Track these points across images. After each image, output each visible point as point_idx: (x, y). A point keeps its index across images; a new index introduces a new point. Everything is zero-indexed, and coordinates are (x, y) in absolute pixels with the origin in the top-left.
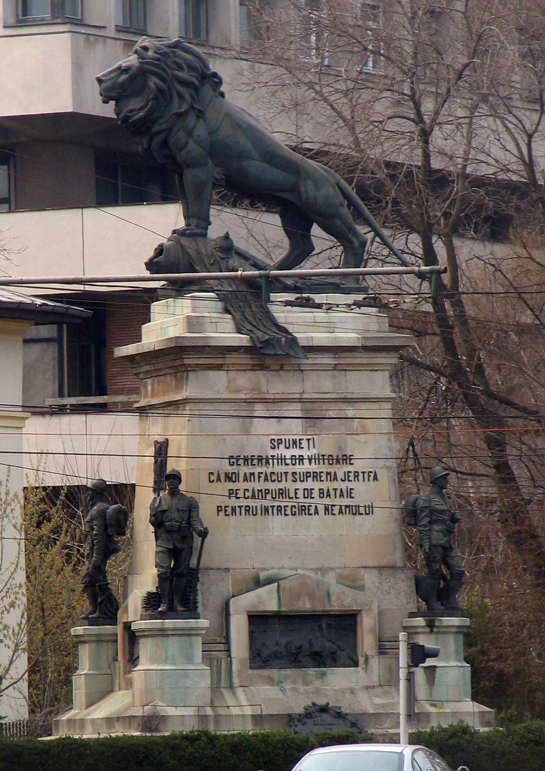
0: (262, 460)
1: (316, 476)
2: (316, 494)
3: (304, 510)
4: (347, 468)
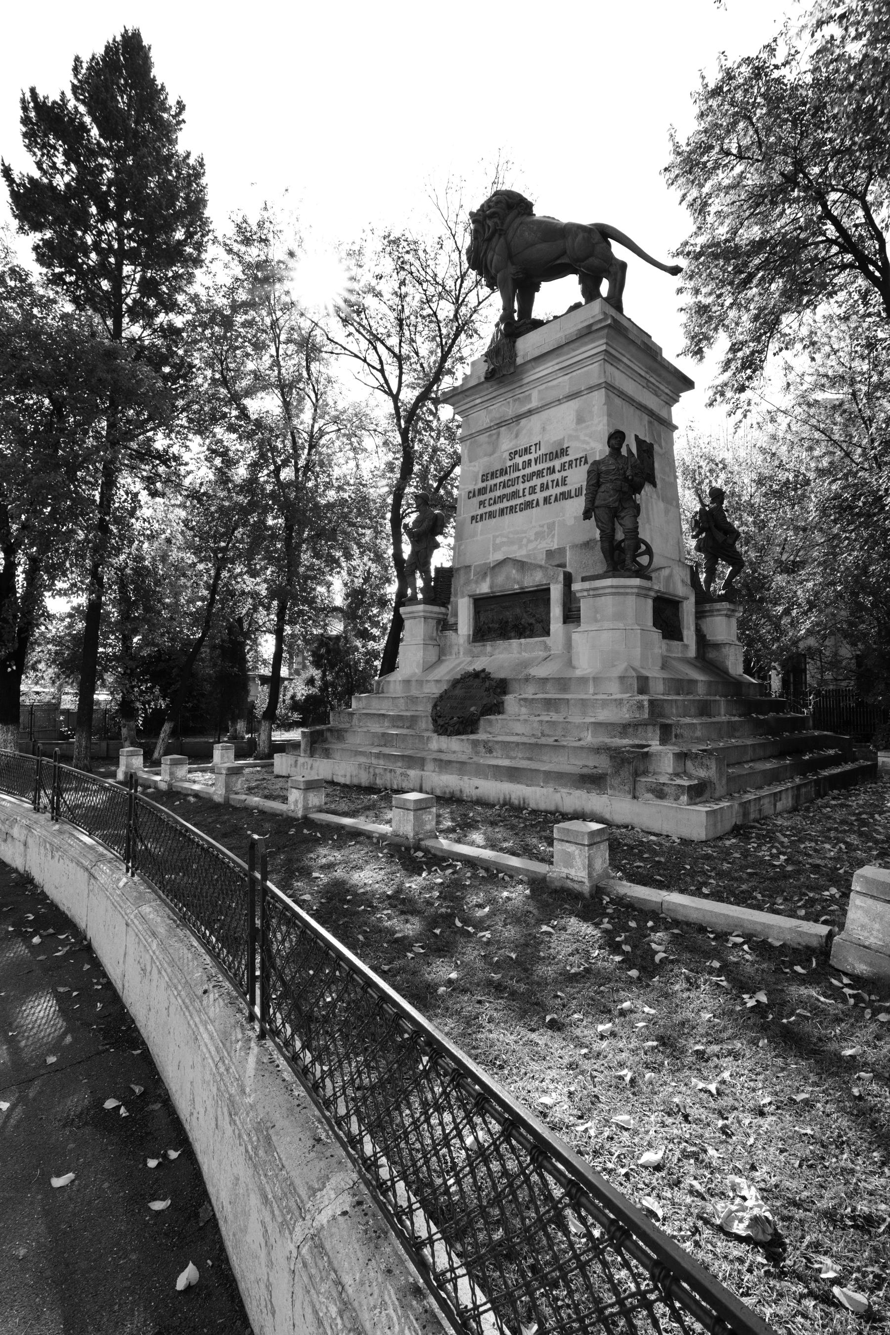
0: (503, 472)
1: (539, 474)
2: (538, 489)
3: (529, 505)
4: (566, 459)
